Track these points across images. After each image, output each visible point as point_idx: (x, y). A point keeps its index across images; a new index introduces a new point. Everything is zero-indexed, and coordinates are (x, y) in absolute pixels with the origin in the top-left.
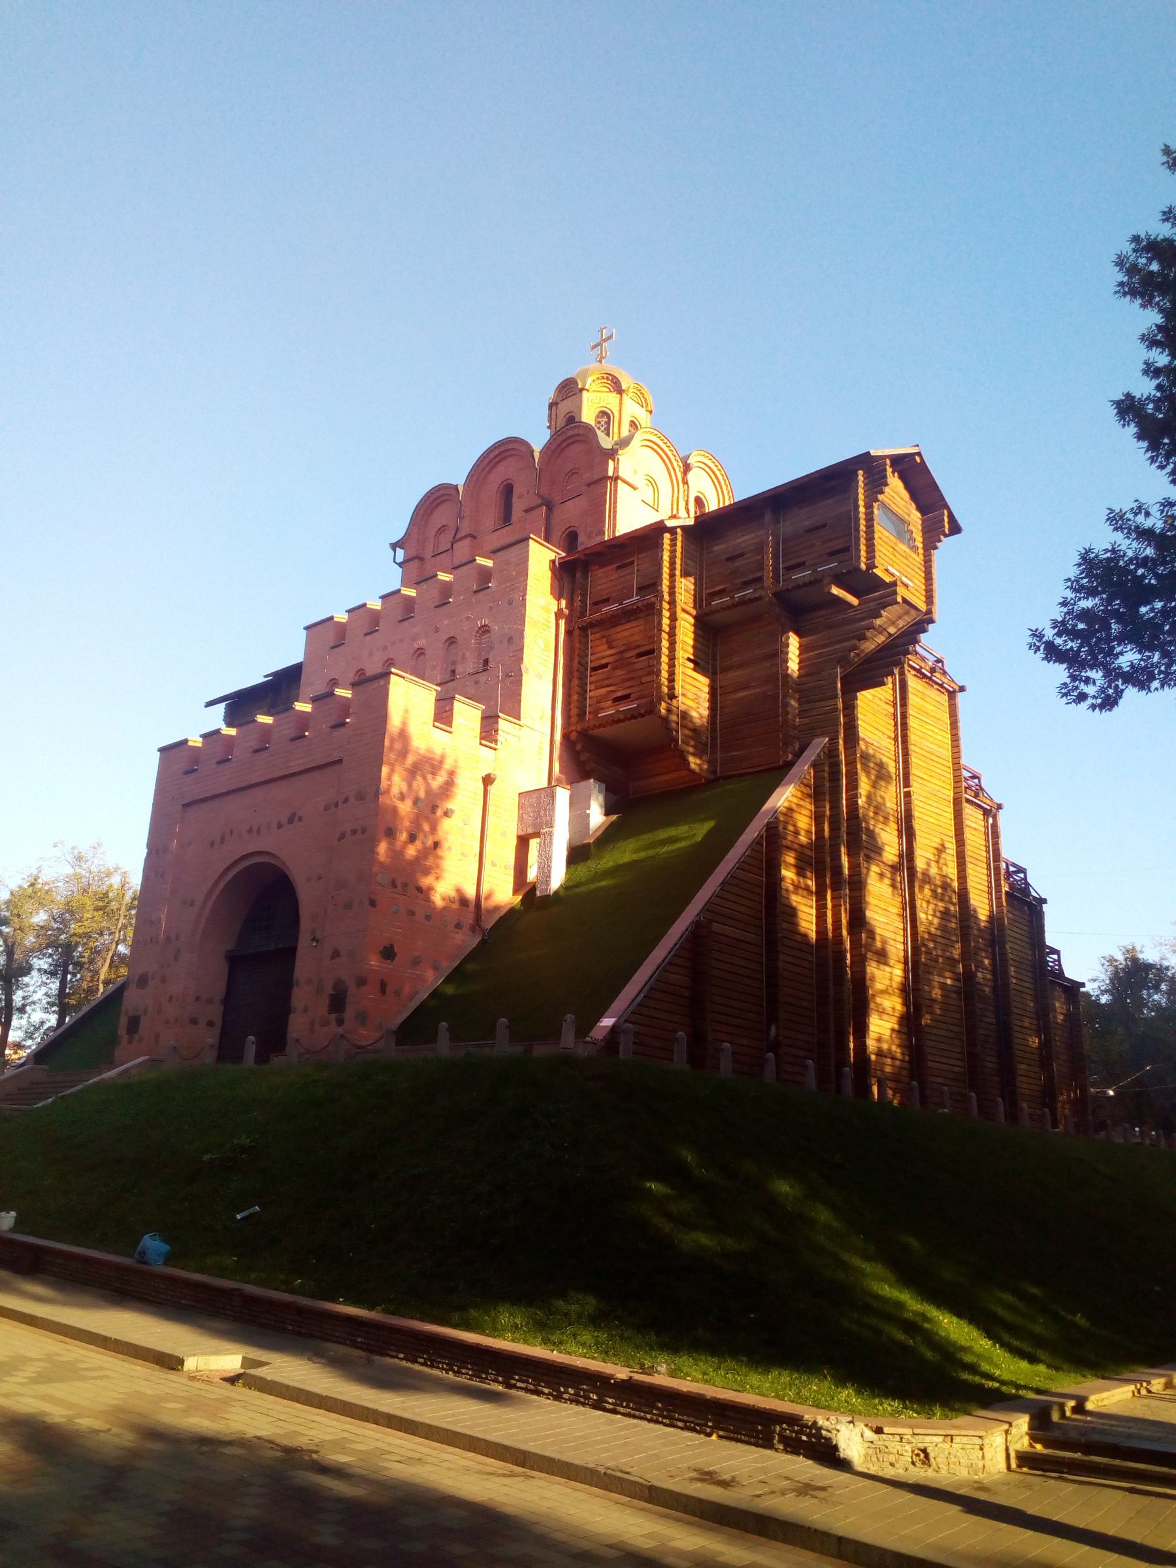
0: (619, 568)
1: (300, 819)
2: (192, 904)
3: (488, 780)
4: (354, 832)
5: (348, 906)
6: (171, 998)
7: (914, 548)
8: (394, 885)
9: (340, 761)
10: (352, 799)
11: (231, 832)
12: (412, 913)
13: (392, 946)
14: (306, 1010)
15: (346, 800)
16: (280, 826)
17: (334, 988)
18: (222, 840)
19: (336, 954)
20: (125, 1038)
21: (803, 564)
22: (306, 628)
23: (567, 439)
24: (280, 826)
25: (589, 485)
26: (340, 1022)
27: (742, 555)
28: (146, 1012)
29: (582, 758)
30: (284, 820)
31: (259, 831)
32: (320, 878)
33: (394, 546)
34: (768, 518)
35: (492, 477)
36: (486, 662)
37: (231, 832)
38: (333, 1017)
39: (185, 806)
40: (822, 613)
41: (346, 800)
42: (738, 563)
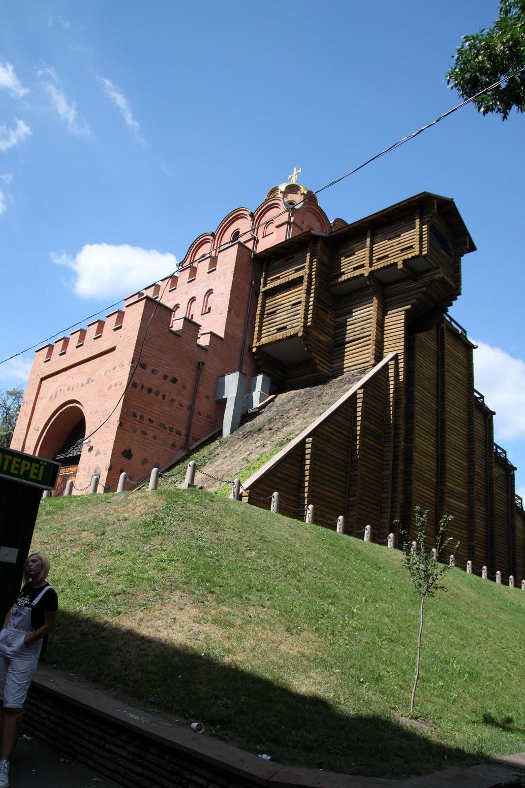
0: (286, 260)
3: (200, 366)
4: (116, 385)
7: (449, 254)
8: (135, 415)
9: (113, 349)
11: (61, 390)
12: (145, 434)
13: (130, 451)
15: (114, 368)
16: (83, 385)
21: (387, 256)
24: (83, 385)
25: (278, 227)
29: (259, 363)
30: (85, 382)
31: (73, 388)
34: (369, 233)
36: (209, 309)
39: (43, 379)
40: (399, 285)
41: (114, 368)
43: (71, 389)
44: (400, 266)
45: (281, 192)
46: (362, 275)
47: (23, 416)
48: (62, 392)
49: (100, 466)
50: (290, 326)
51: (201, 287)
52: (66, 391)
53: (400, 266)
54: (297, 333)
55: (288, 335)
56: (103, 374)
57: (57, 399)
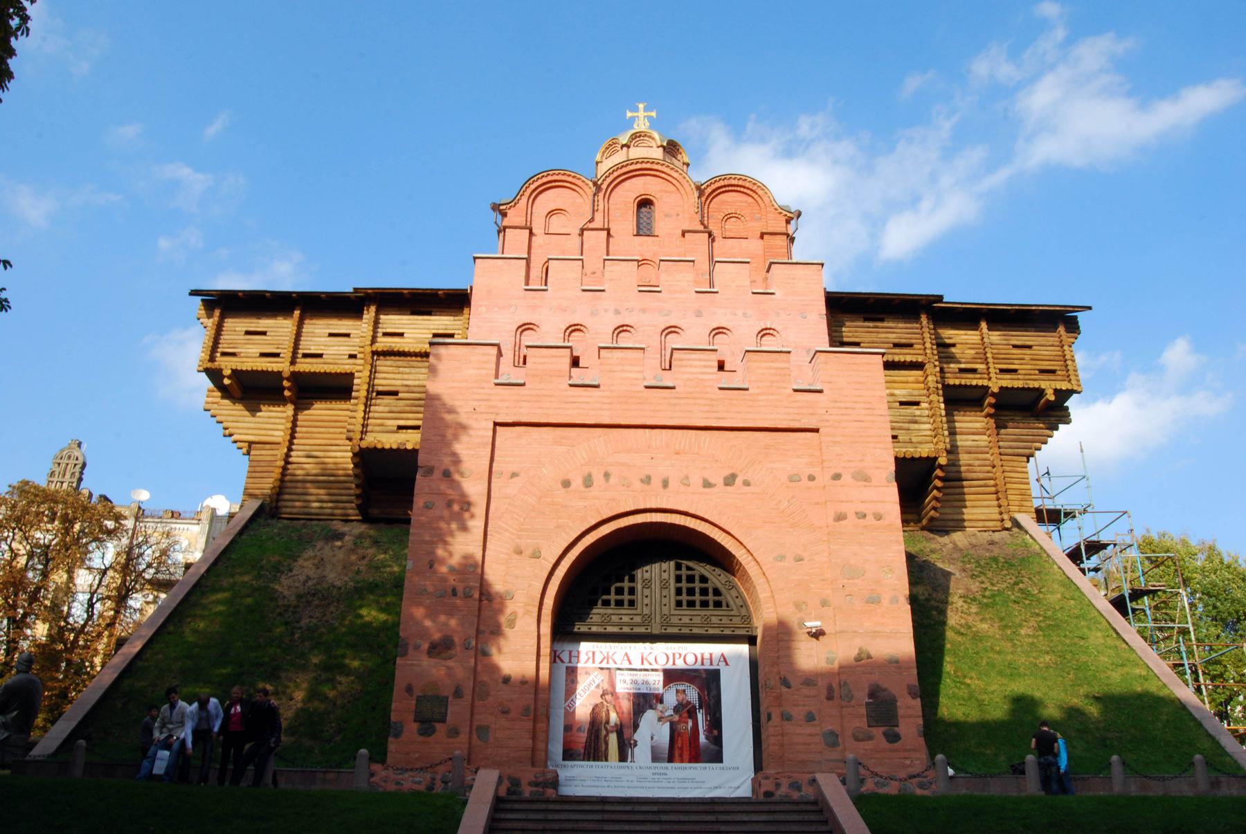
0: (866, 320)
1: (747, 483)
2: (536, 555)
5: (874, 600)
10: (847, 478)
11: (607, 475)
14: (810, 718)
15: (837, 477)
17: (871, 695)
18: (588, 482)
21: (1015, 371)
26: (893, 738)
28: (458, 693)
31: (665, 484)
33: (495, 207)
37: (607, 475)
38: (878, 732)
43: (656, 482)
46: (987, 388)
48: (612, 480)
49: (884, 685)
50: (907, 438)
52: (638, 485)
55: (917, 456)
57: (594, 491)
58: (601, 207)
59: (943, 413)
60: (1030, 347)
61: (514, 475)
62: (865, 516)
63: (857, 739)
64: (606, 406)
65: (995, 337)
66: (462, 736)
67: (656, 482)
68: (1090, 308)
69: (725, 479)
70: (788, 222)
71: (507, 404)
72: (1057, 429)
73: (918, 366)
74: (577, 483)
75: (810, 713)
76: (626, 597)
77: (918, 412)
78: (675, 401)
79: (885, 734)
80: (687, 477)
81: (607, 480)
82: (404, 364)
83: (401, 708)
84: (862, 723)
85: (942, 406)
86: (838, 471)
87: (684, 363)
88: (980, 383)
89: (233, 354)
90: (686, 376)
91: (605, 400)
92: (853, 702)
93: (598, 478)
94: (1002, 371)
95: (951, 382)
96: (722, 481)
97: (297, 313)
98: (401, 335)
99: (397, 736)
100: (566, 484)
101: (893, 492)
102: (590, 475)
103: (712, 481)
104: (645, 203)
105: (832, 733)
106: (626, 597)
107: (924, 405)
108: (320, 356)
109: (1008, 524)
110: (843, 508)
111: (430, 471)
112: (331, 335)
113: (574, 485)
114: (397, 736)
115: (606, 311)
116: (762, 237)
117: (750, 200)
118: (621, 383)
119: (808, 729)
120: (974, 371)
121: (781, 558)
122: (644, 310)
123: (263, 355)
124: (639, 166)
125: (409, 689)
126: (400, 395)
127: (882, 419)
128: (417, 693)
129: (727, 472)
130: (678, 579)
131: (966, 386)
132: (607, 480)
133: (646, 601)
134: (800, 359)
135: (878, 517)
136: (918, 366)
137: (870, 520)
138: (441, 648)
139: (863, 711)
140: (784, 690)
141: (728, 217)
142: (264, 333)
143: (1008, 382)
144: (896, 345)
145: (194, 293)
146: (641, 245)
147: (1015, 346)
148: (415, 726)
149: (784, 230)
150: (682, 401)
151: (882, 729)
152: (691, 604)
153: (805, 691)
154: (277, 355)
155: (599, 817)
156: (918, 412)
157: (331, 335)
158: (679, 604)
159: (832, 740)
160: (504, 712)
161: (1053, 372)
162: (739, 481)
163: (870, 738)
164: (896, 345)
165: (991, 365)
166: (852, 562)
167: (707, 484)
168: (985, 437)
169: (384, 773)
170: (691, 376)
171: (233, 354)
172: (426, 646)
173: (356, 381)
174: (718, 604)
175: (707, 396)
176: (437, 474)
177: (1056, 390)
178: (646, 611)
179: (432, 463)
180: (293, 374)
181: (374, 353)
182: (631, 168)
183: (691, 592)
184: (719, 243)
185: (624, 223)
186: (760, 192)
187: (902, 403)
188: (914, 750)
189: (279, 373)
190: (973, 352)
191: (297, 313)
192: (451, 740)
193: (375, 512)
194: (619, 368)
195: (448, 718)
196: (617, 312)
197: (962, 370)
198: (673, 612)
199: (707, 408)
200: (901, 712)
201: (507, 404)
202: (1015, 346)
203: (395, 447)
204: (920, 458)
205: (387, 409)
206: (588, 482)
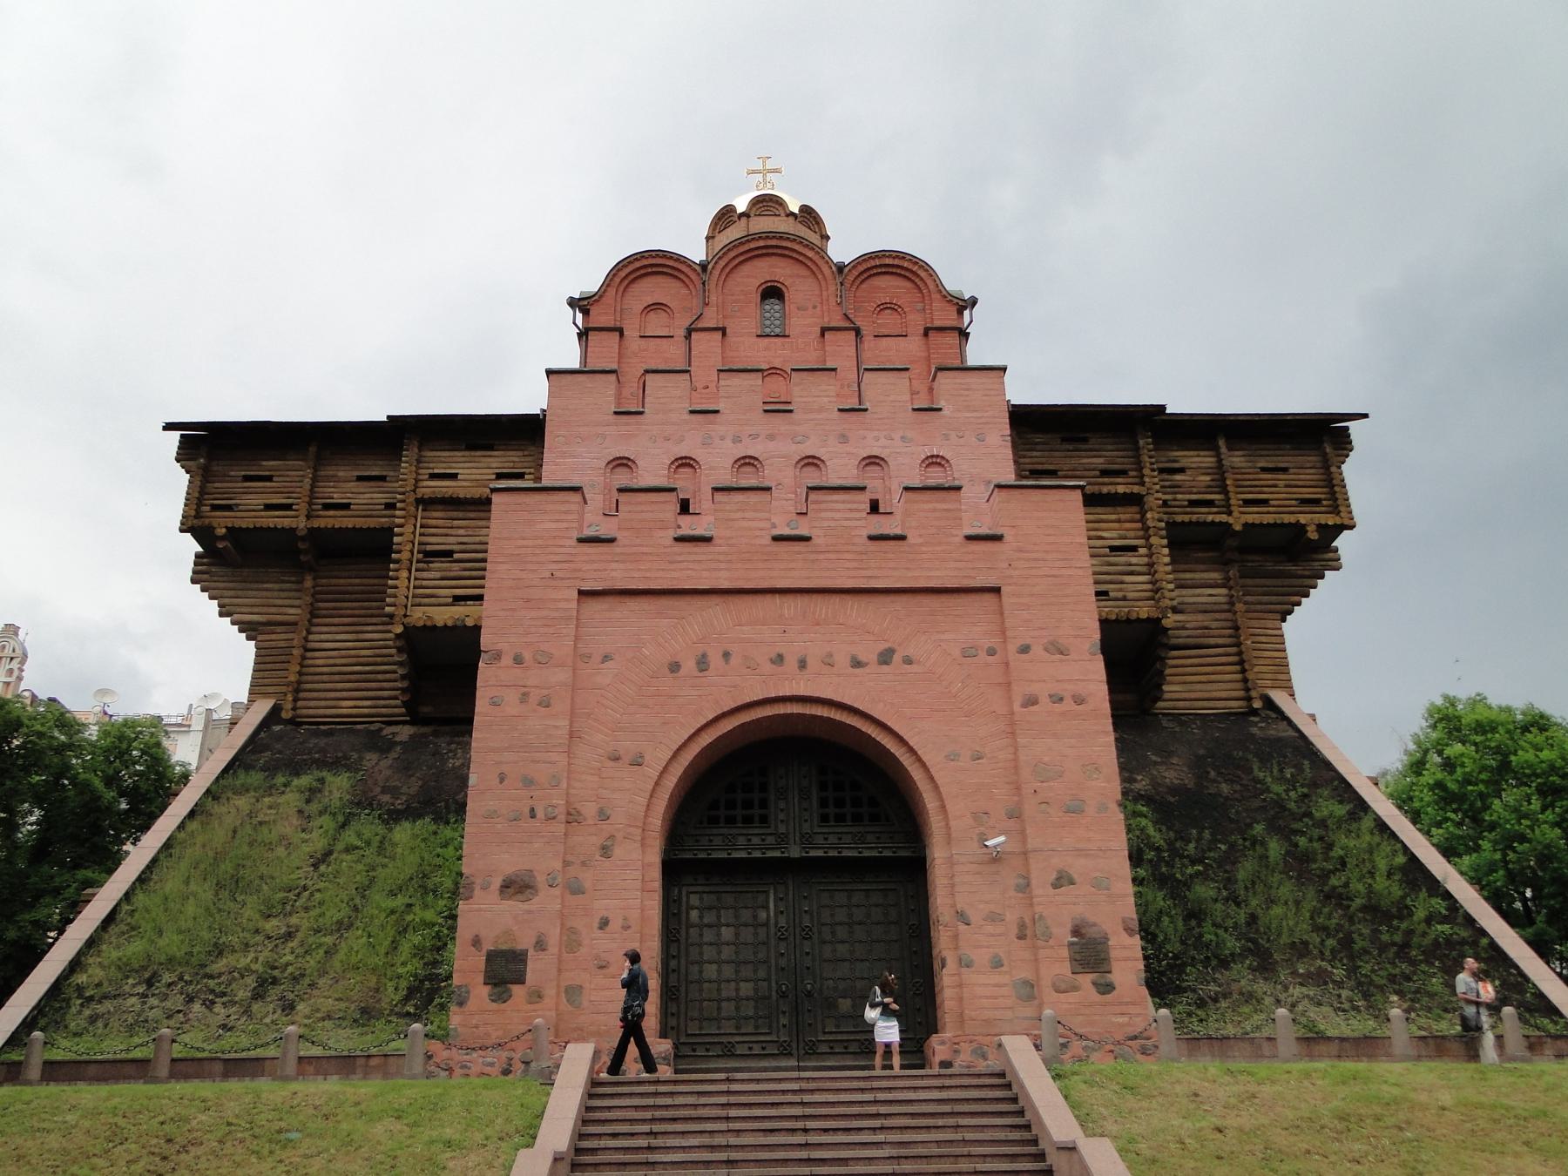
0: (1063, 440)
1: (908, 661)
5: (1075, 809)
6: (604, 923)
10: (1037, 650)
11: (726, 655)
14: (997, 964)
15: (1025, 649)
17: (1076, 932)
18: (703, 663)
19: (1063, 880)
20: (480, 992)
21: (1265, 502)
22: (549, 372)
23: (881, 266)
24: (857, 664)
26: (1106, 988)
27: (1182, 470)
28: (540, 945)
30: (869, 654)
31: (803, 664)
32: (978, 757)
33: (572, 303)
35: (746, 268)
37: (726, 655)
38: (1086, 980)
42: (1178, 477)
43: (791, 662)
44: (1313, 535)
45: (792, 214)
47: (511, 696)
48: (734, 660)
49: (1092, 919)
50: (1120, 595)
51: (897, 436)
52: (768, 667)
53: (1313, 535)
54: (1159, 620)
55: (1134, 616)
56: (957, 653)
58: (713, 298)
59: (1167, 560)
60: (1285, 470)
61: (606, 658)
62: (1061, 699)
63: (1058, 991)
64: (723, 566)
65: (1235, 459)
66: (546, 1000)
67: (791, 662)
68: (1365, 416)
69: (881, 654)
70: (960, 312)
71: (595, 566)
72: (1322, 577)
73: (1135, 500)
74: (689, 666)
75: (997, 955)
76: (756, 812)
77: (1134, 560)
78: (813, 556)
79: (1094, 984)
80: (830, 655)
81: (727, 662)
82: (461, 514)
83: (466, 965)
84: (1065, 969)
85: (1166, 551)
86: (1028, 641)
87: (823, 506)
88: (1218, 518)
89: (229, 508)
90: (826, 524)
91: (721, 558)
92: (1051, 942)
93: (715, 660)
94: (1247, 503)
95: (1179, 518)
96: (873, 657)
97: (313, 449)
98: (454, 476)
99: (461, 1004)
100: (675, 667)
101: (1098, 667)
102: (704, 656)
103: (862, 658)
104: (772, 293)
105: (1028, 984)
106: (756, 812)
107: (1142, 551)
108: (346, 506)
109: (1257, 704)
110: (1035, 689)
111: (498, 656)
112: (360, 478)
113: (682, 672)
114: (461, 1004)
115: (722, 438)
116: (926, 334)
117: (909, 285)
118: (741, 537)
119: (996, 978)
120: (1210, 503)
121: (951, 758)
122: (771, 437)
123: (268, 507)
124: (762, 243)
125: (476, 942)
126: (456, 556)
127: (1080, 572)
128: (488, 946)
129: (883, 646)
130: (823, 787)
131: (1198, 523)
132: (727, 662)
133: (782, 816)
134: (974, 494)
135: (1079, 700)
136: (1135, 500)
137: (1068, 705)
138: (516, 887)
139: (1065, 953)
140: (962, 927)
141: (884, 307)
142: (269, 479)
143: (1254, 516)
144: (1105, 473)
145: (169, 427)
146: (766, 349)
147: (1264, 470)
148: (486, 990)
149: (954, 324)
150: (822, 557)
151: (1091, 976)
152: (840, 819)
153: (990, 929)
154: (288, 507)
155: (723, 1100)
156: (1134, 560)
157: (360, 478)
158: (824, 819)
159: (1029, 991)
160: (601, 967)
161: (1317, 502)
162: (897, 658)
163: (1075, 988)
164: (1105, 473)
165: (1232, 495)
166: (1046, 759)
167: (857, 664)
168: (1224, 591)
169: (446, 1054)
170: (832, 524)
171: (229, 508)
172: (497, 882)
173: (396, 539)
174: (874, 818)
175: (855, 548)
176: (507, 660)
177: (1319, 526)
178: (782, 829)
179: (499, 646)
180: (311, 530)
181: (419, 501)
182: (752, 245)
183: (840, 803)
184: (869, 342)
185: (746, 318)
186: (923, 274)
187: (1113, 549)
188: (1133, 1004)
189: (293, 530)
190: (1208, 478)
191: (313, 449)
192: (530, 1007)
193: (426, 710)
194: (739, 515)
195: (529, 976)
196: (737, 440)
197: (1193, 503)
198: (817, 830)
199: (855, 564)
200: (1113, 954)
201: (595, 566)
202: (1264, 470)
203: (450, 624)
204: (1138, 620)
205: (438, 575)
206: (703, 663)
